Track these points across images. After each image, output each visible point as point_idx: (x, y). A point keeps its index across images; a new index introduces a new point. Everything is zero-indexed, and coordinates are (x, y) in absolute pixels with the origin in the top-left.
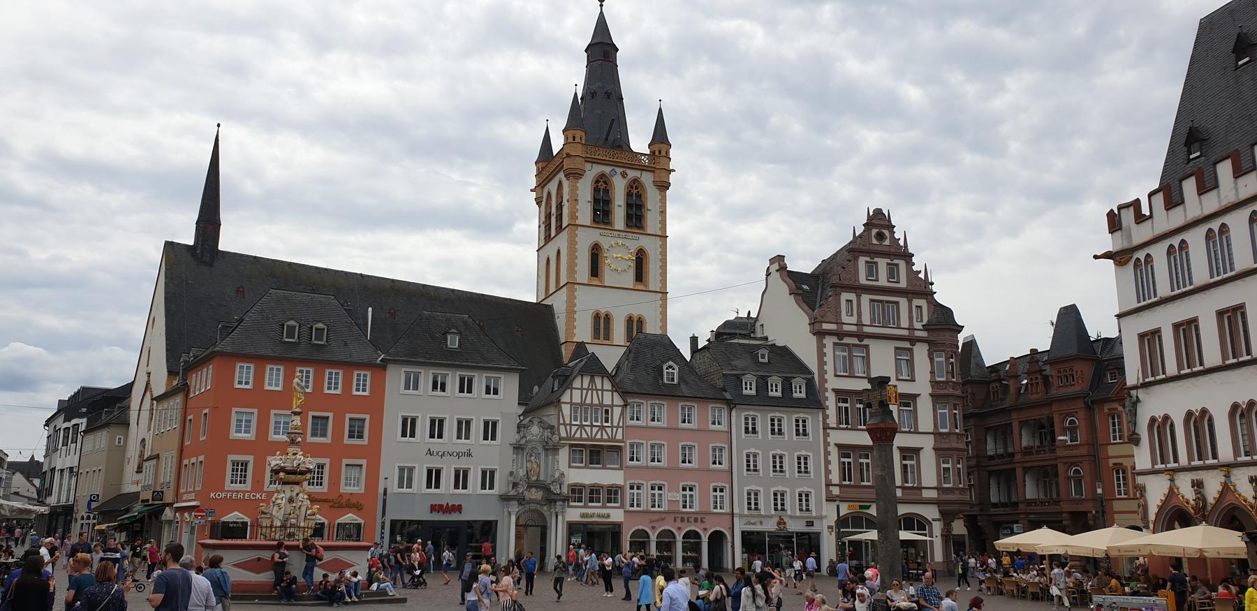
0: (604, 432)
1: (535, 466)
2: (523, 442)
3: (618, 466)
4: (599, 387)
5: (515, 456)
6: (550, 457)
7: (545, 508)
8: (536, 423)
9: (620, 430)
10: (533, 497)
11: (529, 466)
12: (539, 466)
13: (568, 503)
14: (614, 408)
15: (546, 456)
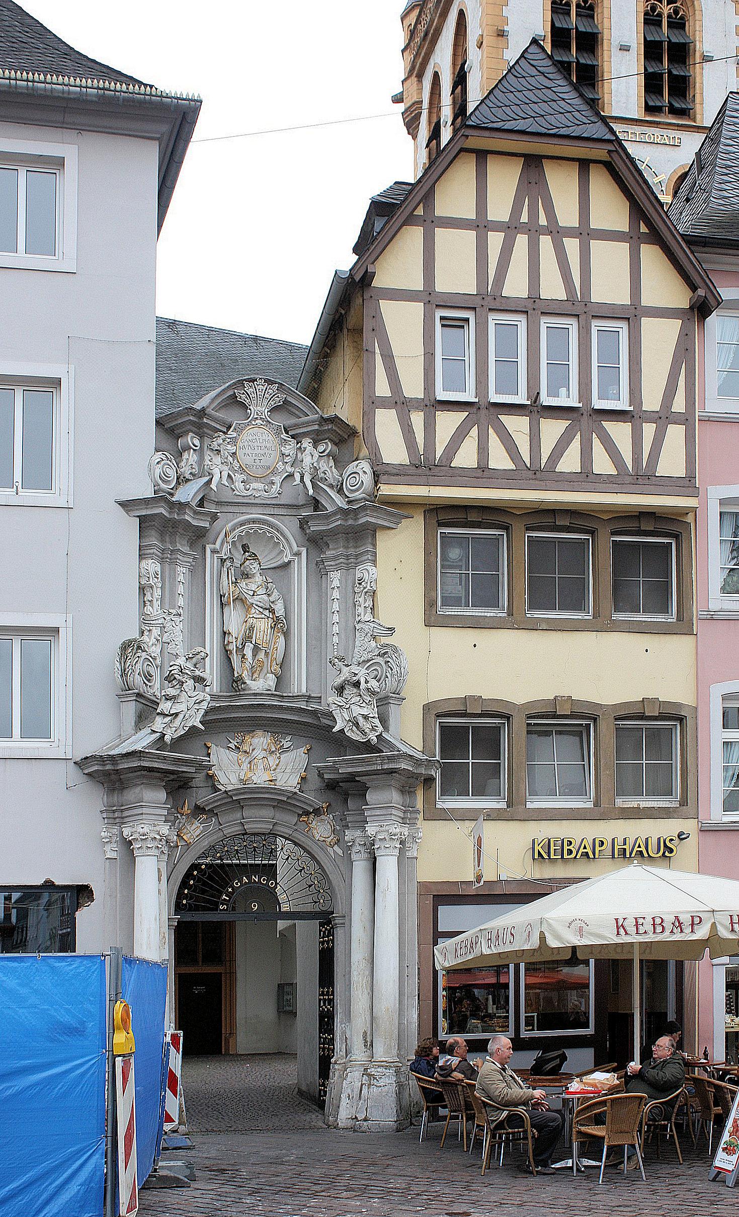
0: (596, 442)
1: (262, 626)
2: (187, 494)
3: (673, 619)
4: (568, 216)
5: (152, 566)
6: (336, 578)
7: (321, 829)
8: (259, 408)
9: (675, 434)
10: (260, 778)
11: (235, 622)
12: (281, 625)
13: (430, 802)
14: (646, 323)
15: (319, 571)
